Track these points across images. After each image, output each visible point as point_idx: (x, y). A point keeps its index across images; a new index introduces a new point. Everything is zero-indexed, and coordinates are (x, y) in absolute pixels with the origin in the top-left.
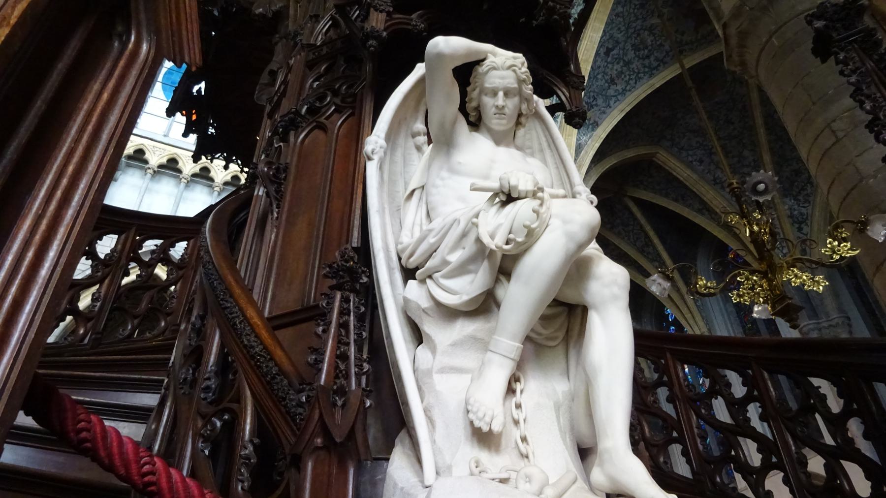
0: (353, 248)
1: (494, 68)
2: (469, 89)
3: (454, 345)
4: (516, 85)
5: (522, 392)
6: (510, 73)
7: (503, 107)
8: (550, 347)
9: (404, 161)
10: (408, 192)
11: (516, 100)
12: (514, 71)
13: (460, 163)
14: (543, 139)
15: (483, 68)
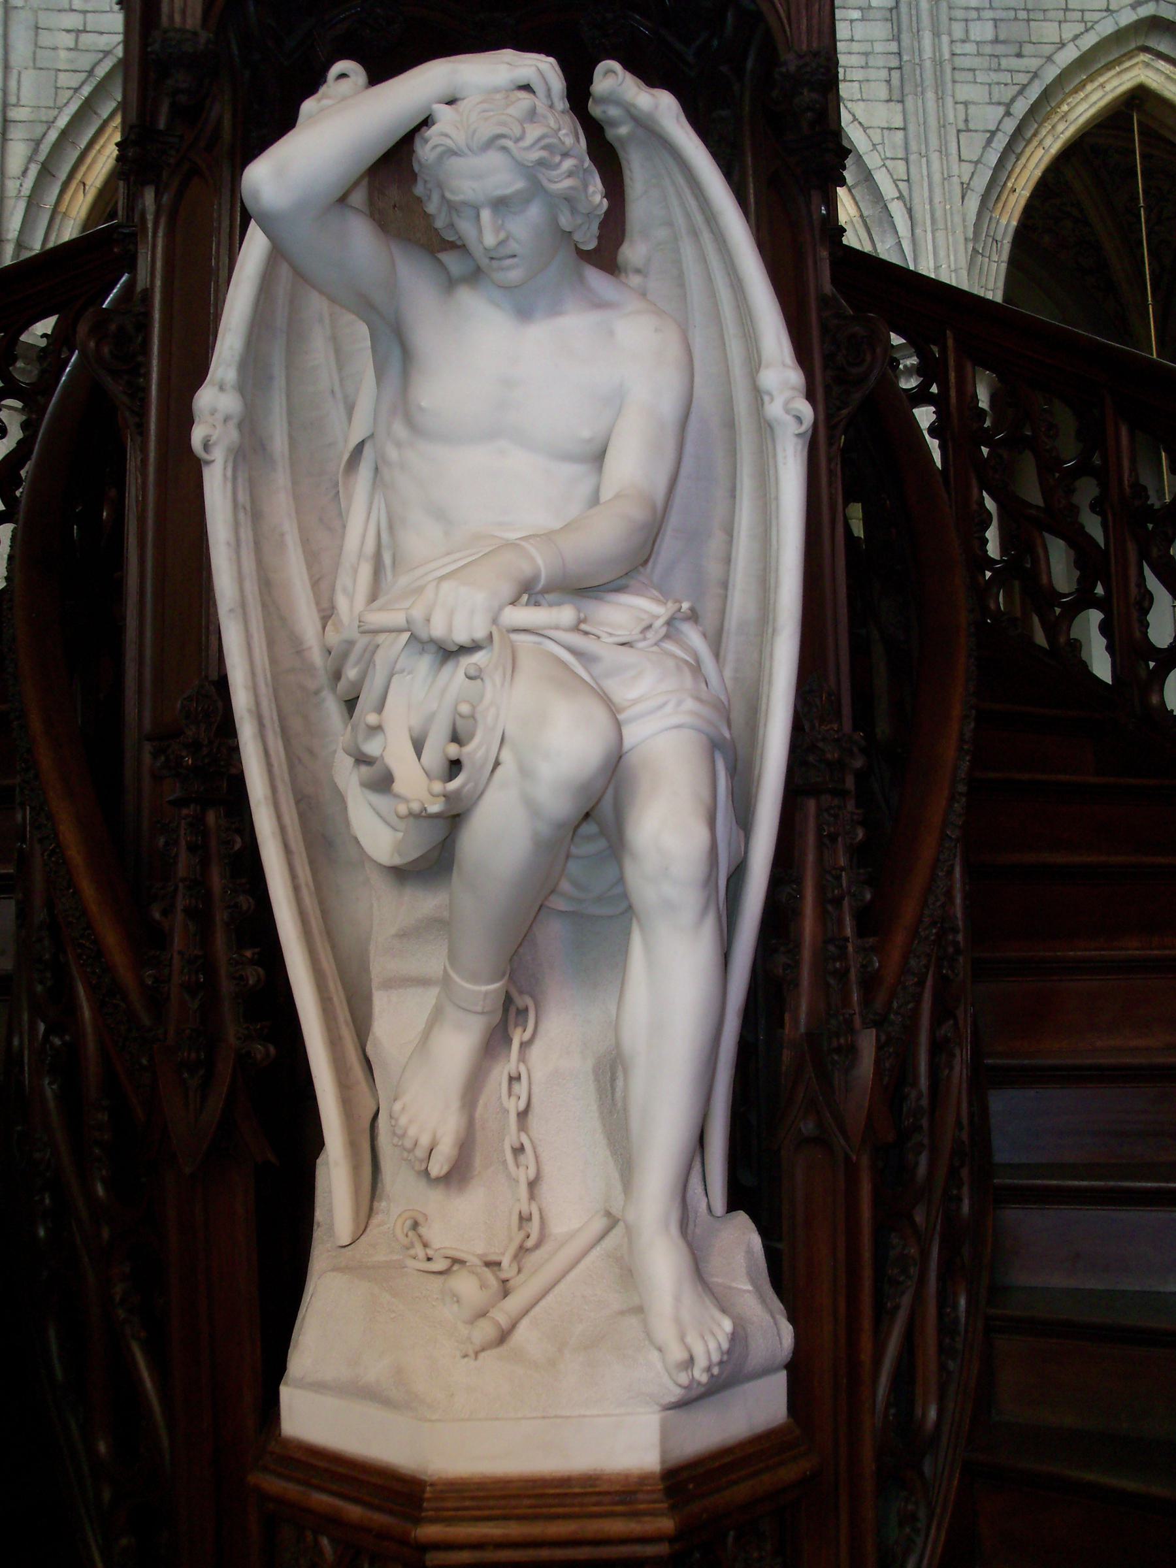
0: (213, 683)
1: (453, 153)
2: (419, 190)
3: (403, 935)
4: (520, 184)
5: (525, 1045)
6: (494, 158)
7: (501, 243)
8: (610, 917)
9: (338, 351)
10: (346, 457)
11: (535, 211)
12: (504, 149)
13: (421, 409)
14: (692, 204)
15: (426, 151)
